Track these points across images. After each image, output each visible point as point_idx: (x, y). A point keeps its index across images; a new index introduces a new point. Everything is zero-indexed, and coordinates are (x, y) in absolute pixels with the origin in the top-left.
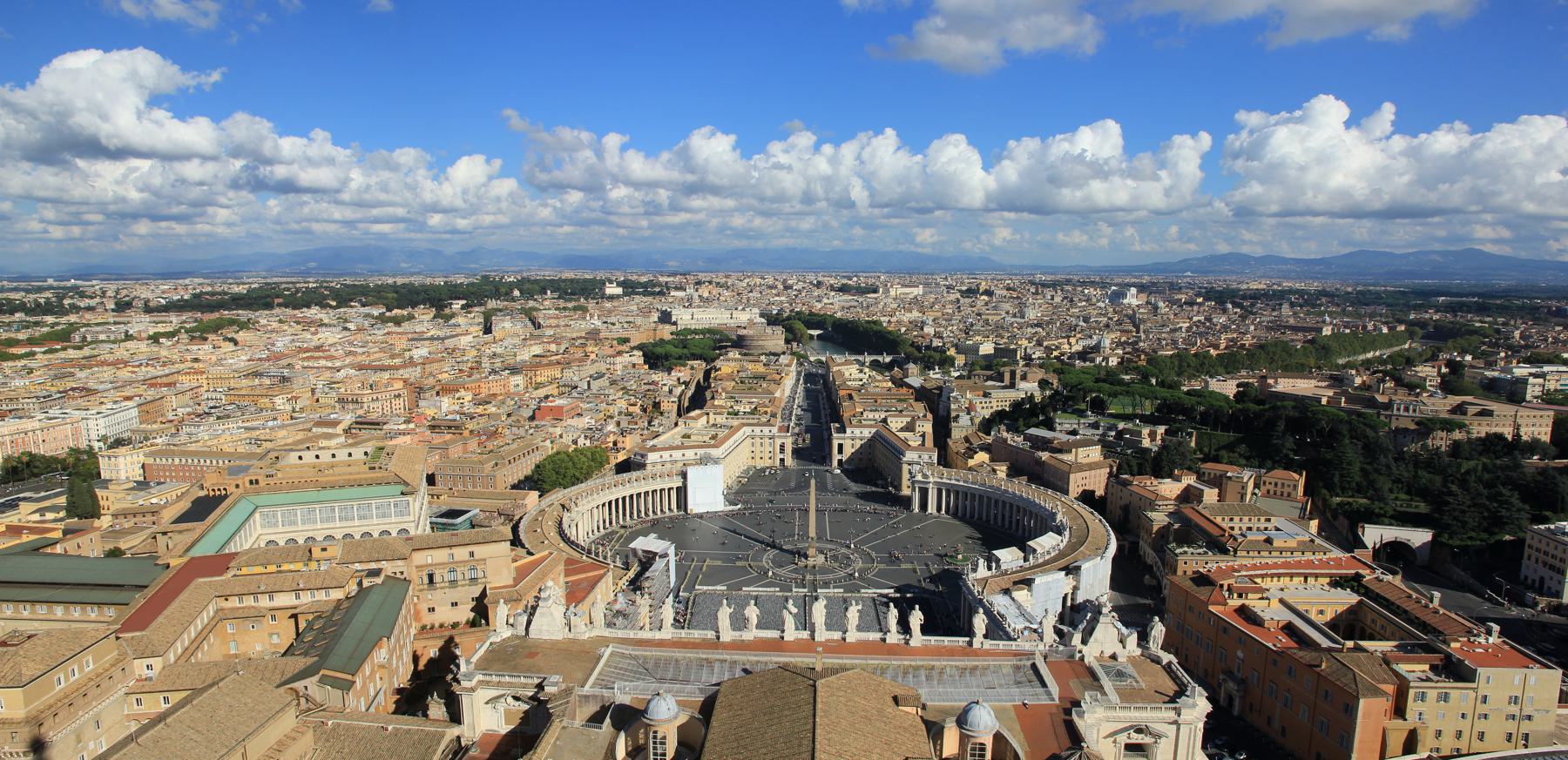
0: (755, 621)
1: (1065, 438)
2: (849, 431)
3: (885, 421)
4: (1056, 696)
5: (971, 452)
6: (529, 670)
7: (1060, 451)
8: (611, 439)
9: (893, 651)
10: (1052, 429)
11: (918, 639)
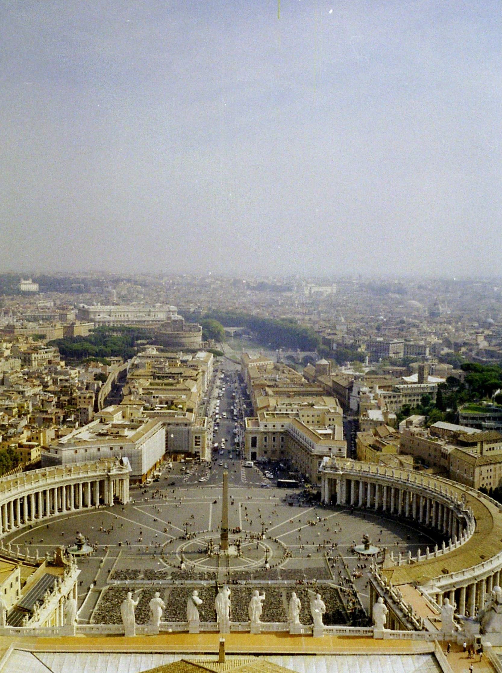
0: (160, 613)
3: (297, 415)
8: (27, 434)
10: (457, 423)
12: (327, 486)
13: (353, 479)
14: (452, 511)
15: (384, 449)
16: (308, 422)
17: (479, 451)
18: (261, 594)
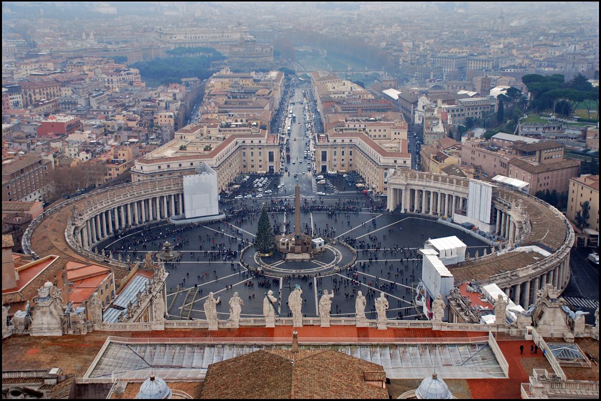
1: (530, 140)
2: (331, 140)
3: (364, 129)
4: (506, 372)
5: (439, 158)
6: (28, 365)
7: (524, 153)
9: (363, 332)
10: (517, 134)
11: (383, 322)
12: (392, 195)
13: (416, 188)
14: (510, 216)
15: (446, 161)
16: (375, 136)
17: (537, 160)
18: (330, 293)
